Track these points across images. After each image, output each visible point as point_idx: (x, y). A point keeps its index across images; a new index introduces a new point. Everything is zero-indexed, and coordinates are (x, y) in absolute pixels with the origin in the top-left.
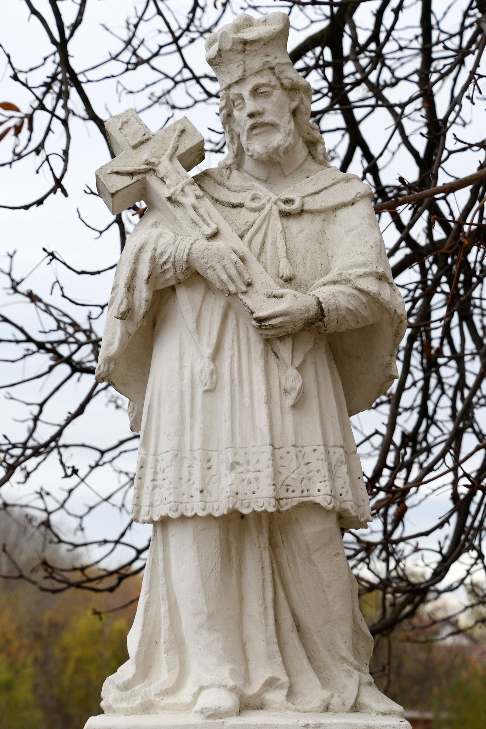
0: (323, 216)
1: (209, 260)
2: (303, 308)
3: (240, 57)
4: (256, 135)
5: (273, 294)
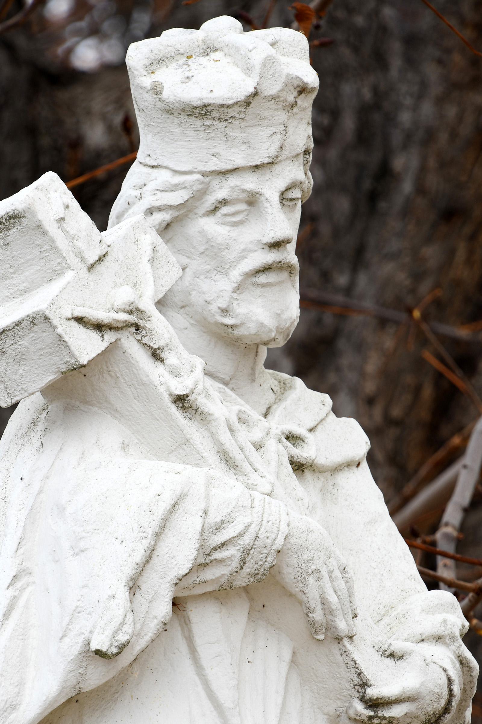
3: (282, 116)
5: (392, 648)
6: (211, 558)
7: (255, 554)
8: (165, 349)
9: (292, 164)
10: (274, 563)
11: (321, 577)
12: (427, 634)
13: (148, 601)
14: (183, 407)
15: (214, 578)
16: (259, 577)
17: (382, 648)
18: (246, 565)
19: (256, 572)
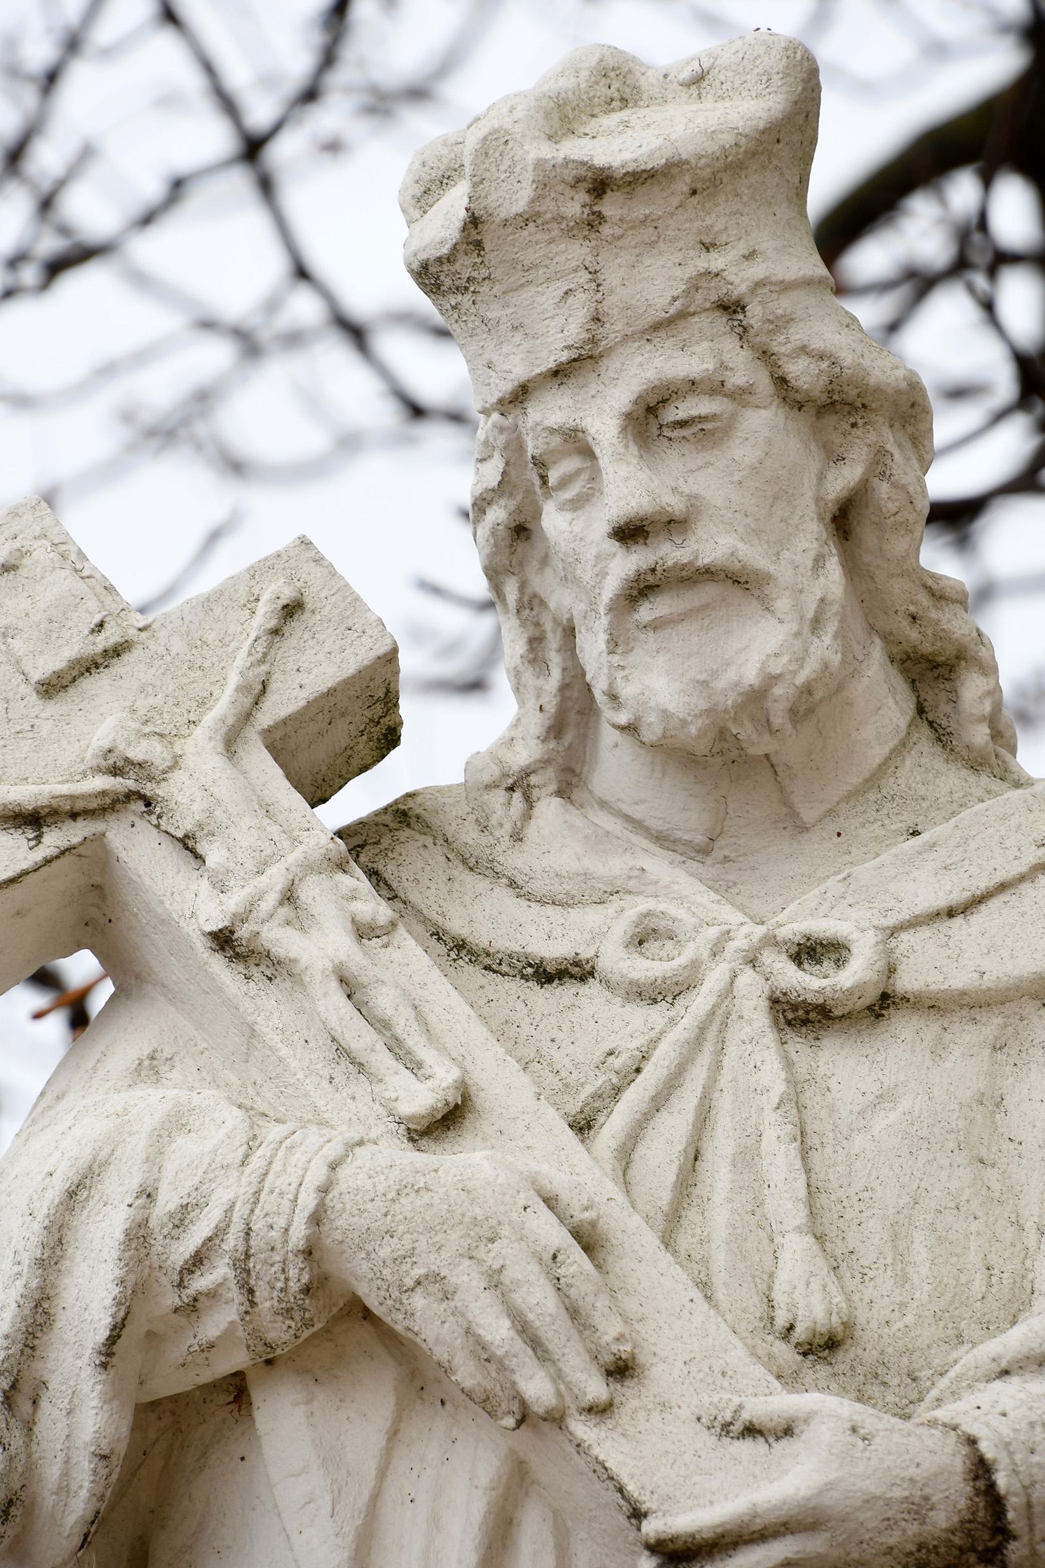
0: (991, 1026)
1: (422, 1246)
2: (898, 1493)
3: (576, 252)
4: (655, 626)
5: (746, 1415)
6: (191, 1291)
7: (258, 1267)
8: (198, 835)
9: (649, 347)
10: (304, 1281)
11: (451, 1289)
12: (1009, 1357)
13: (64, 1412)
14: (237, 956)
15: (218, 1333)
16: (297, 1315)
17: (719, 1418)
18: (257, 1294)
19: (283, 1305)
